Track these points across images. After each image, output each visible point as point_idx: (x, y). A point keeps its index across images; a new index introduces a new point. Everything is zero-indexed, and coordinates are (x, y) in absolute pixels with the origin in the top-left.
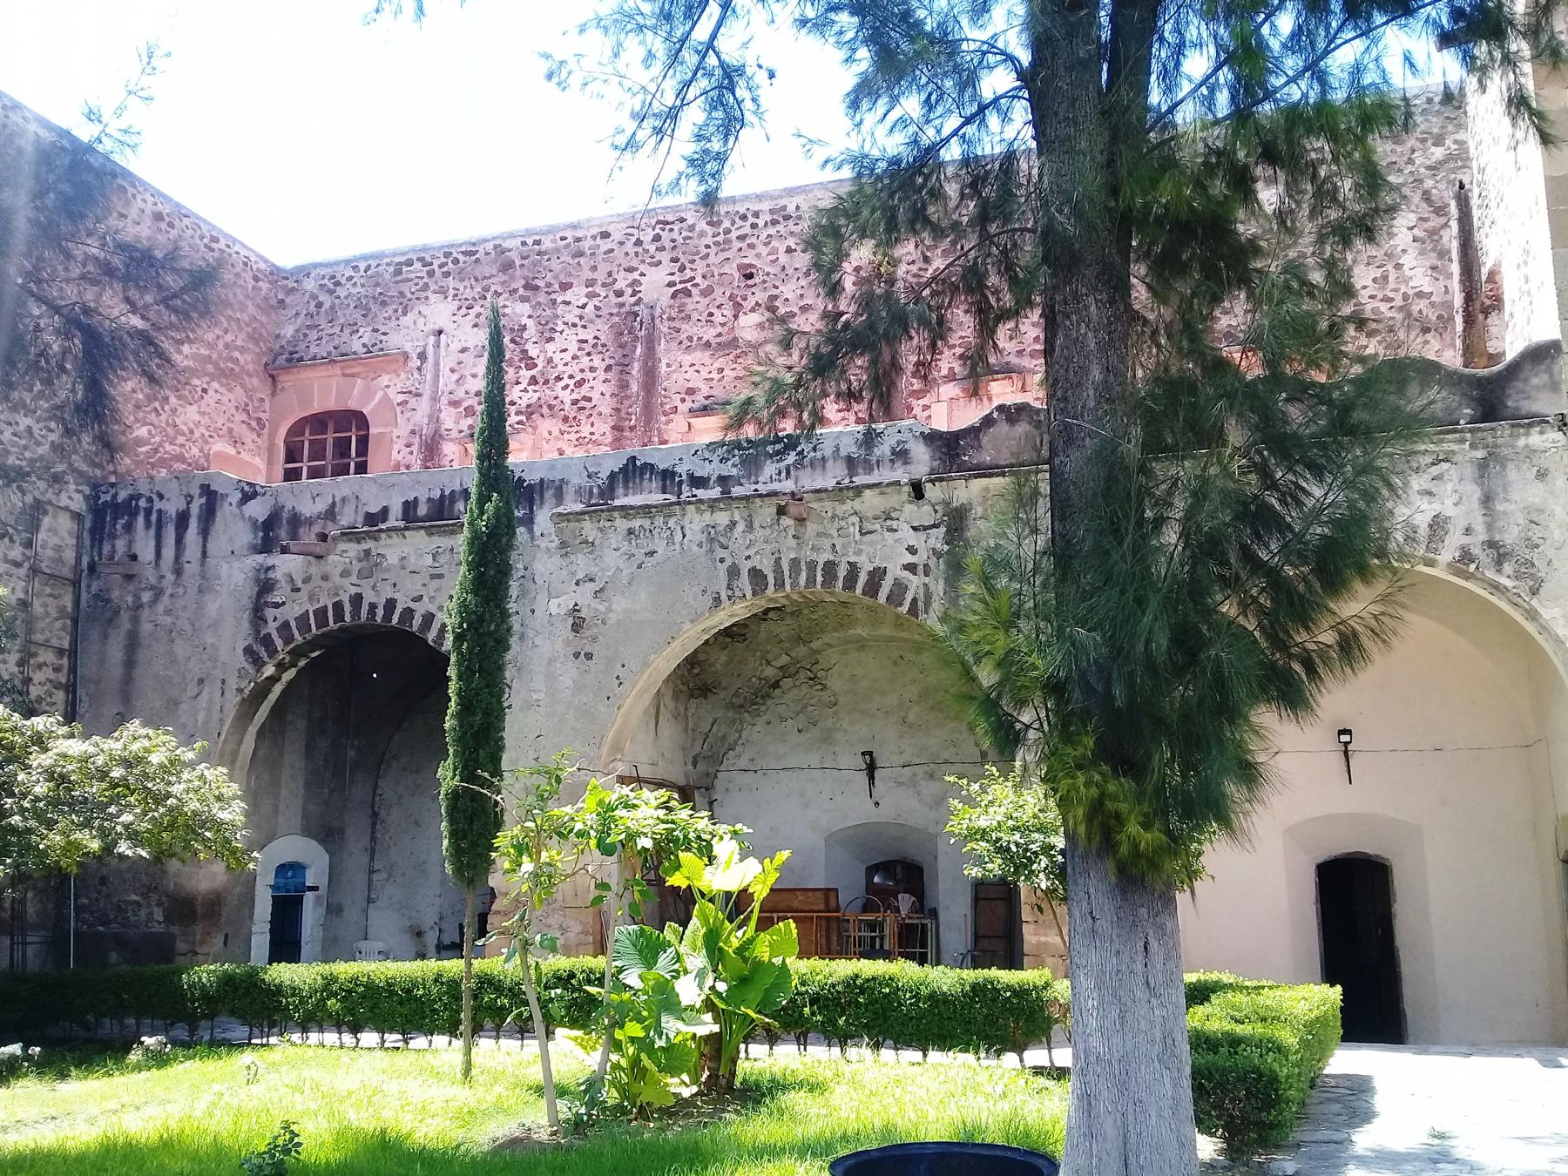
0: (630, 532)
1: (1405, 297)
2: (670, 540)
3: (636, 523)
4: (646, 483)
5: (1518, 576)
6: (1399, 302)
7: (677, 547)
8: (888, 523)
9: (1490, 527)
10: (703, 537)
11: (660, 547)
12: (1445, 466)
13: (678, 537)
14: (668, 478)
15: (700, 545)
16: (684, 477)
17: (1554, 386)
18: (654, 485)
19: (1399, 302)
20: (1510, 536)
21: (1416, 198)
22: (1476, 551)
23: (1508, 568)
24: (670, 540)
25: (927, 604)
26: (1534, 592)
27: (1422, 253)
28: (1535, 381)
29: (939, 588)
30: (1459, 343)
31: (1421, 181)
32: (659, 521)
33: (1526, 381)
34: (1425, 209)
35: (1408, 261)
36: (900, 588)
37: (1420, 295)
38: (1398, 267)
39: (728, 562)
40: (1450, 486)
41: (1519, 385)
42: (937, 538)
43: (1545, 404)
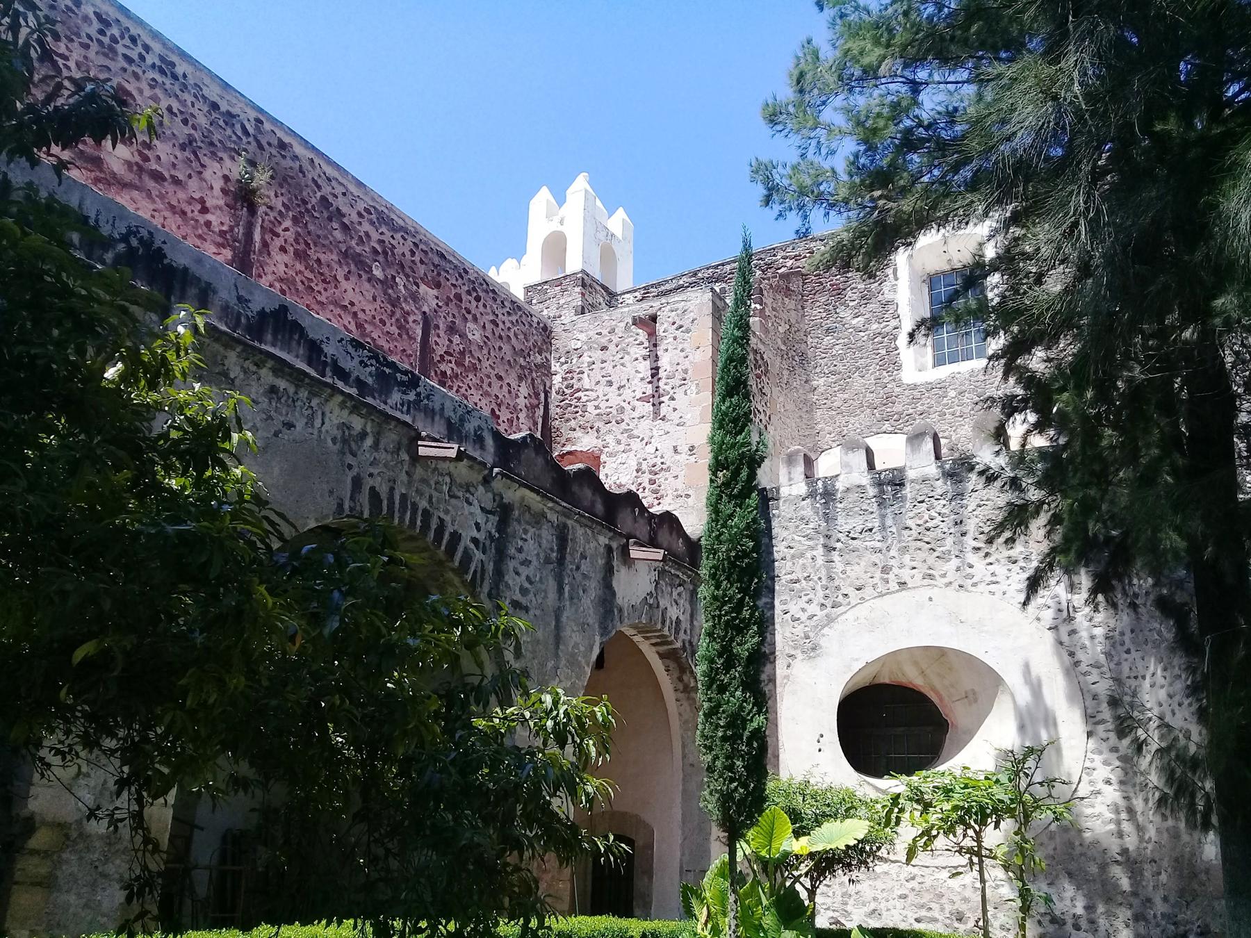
0: (273, 390)
2: (310, 420)
3: (282, 384)
4: (294, 344)
7: (316, 432)
8: (468, 495)
10: (339, 434)
11: (300, 425)
13: (318, 423)
14: (314, 351)
15: (334, 440)
16: (329, 360)
18: (301, 352)
24: (310, 420)
25: (482, 579)
29: (490, 567)
32: (304, 394)
36: (467, 557)
39: (355, 471)
42: (491, 524)
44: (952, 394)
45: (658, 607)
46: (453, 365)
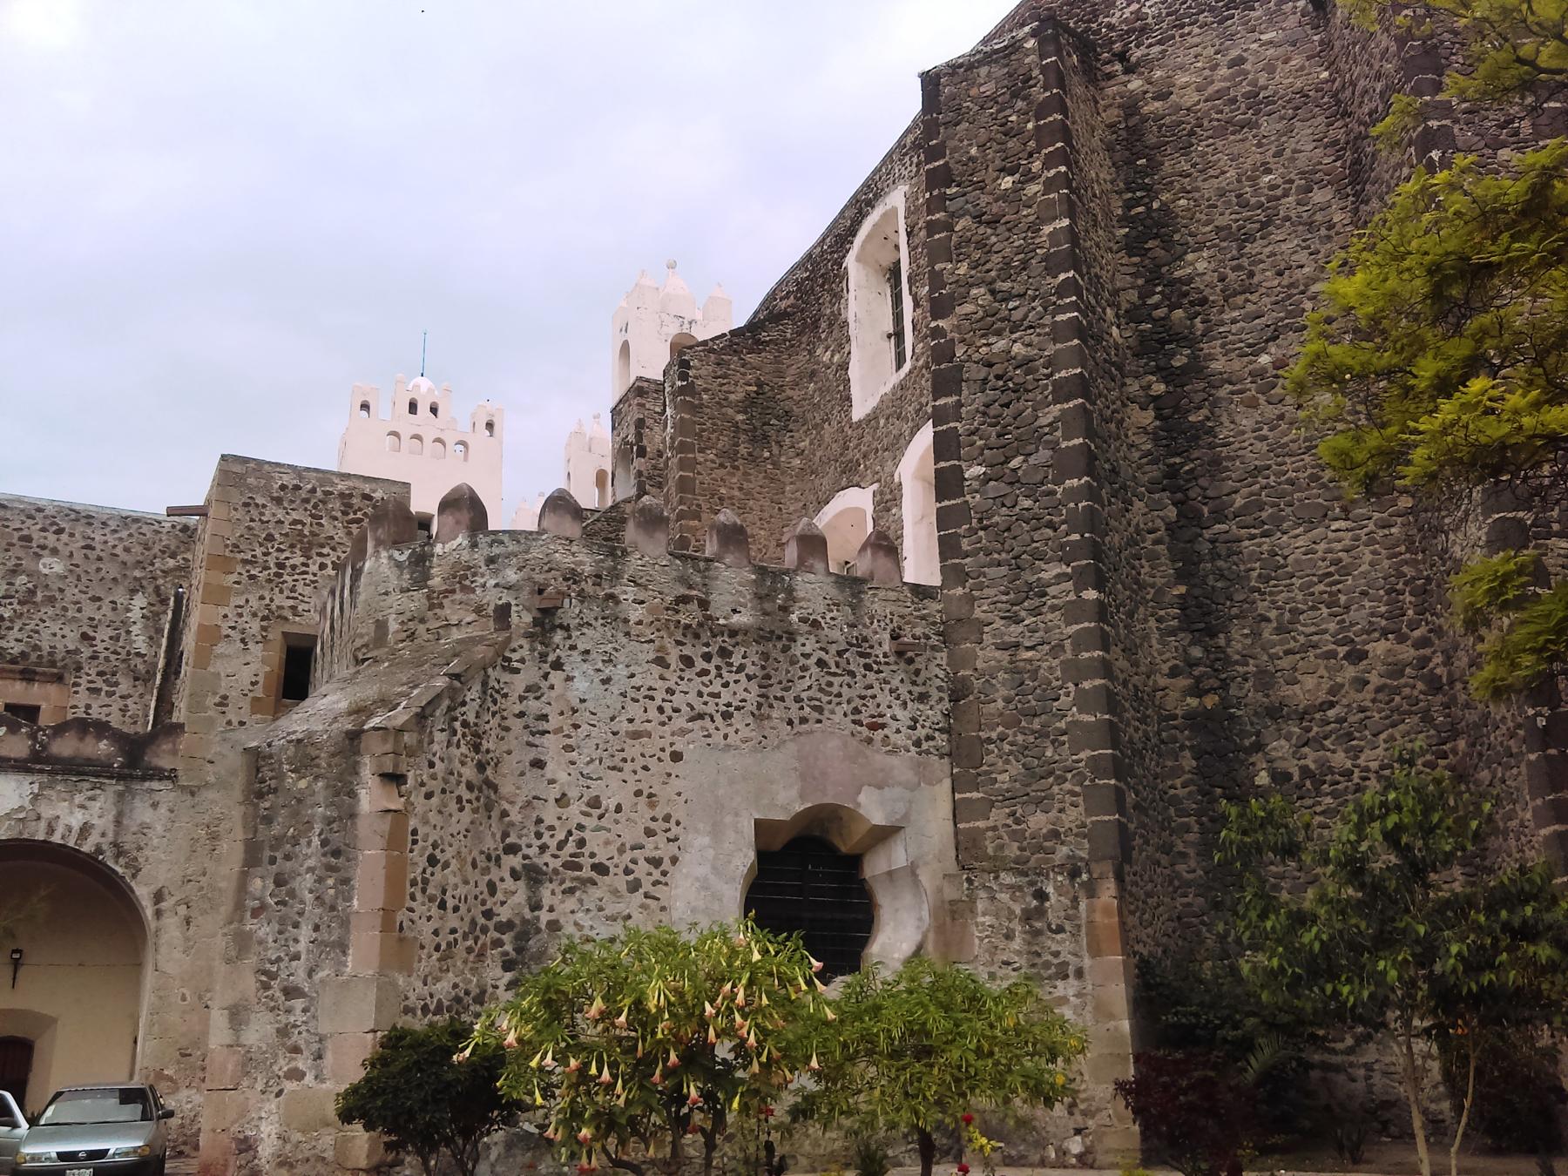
1: (129, 653)
5: (127, 866)
6: (123, 656)
9: (117, 834)
12: (98, 792)
17: (174, 752)
19: (123, 656)
20: (128, 841)
21: (150, 589)
22: (105, 847)
23: (122, 861)
26: (134, 876)
27: (146, 627)
28: (164, 747)
30: (155, 691)
31: (155, 578)
33: (159, 746)
34: (153, 599)
35: (135, 629)
37: (138, 654)
38: (128, 632)
40: (98, 805)
41: (154, 747)
43: (165, 762)
44: (882, 422)
45: (39, 818)
46: (16, 606)
